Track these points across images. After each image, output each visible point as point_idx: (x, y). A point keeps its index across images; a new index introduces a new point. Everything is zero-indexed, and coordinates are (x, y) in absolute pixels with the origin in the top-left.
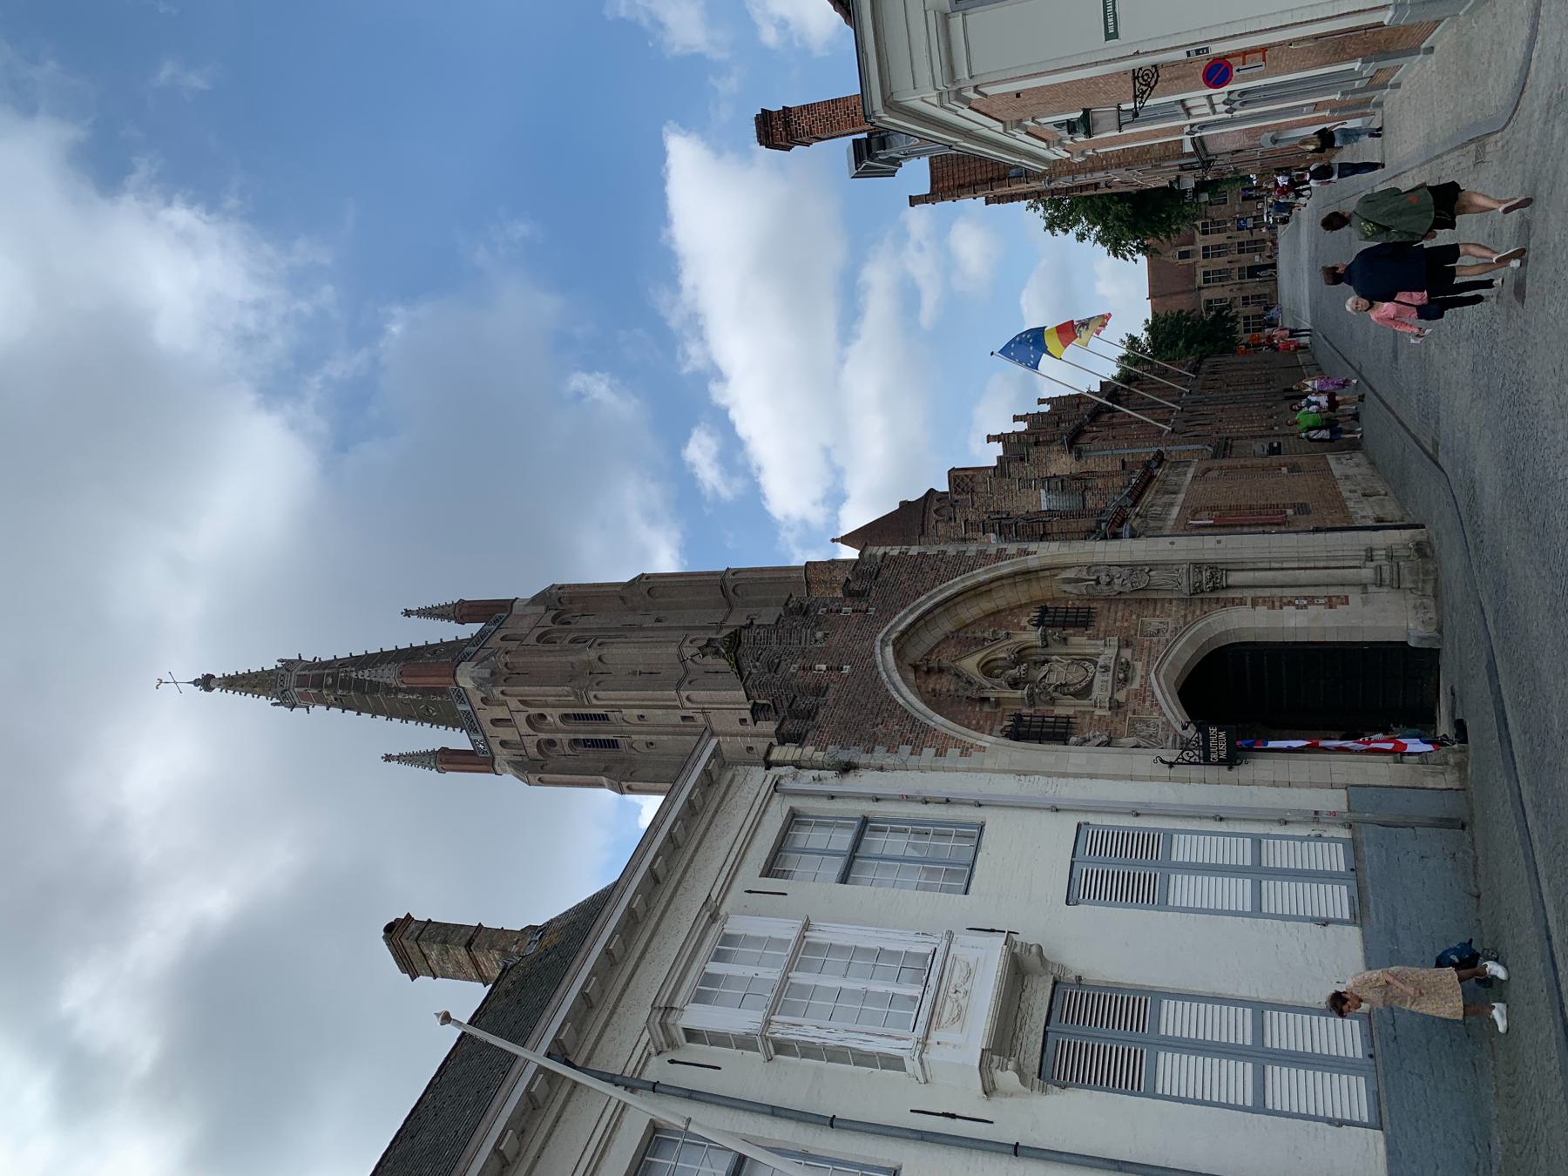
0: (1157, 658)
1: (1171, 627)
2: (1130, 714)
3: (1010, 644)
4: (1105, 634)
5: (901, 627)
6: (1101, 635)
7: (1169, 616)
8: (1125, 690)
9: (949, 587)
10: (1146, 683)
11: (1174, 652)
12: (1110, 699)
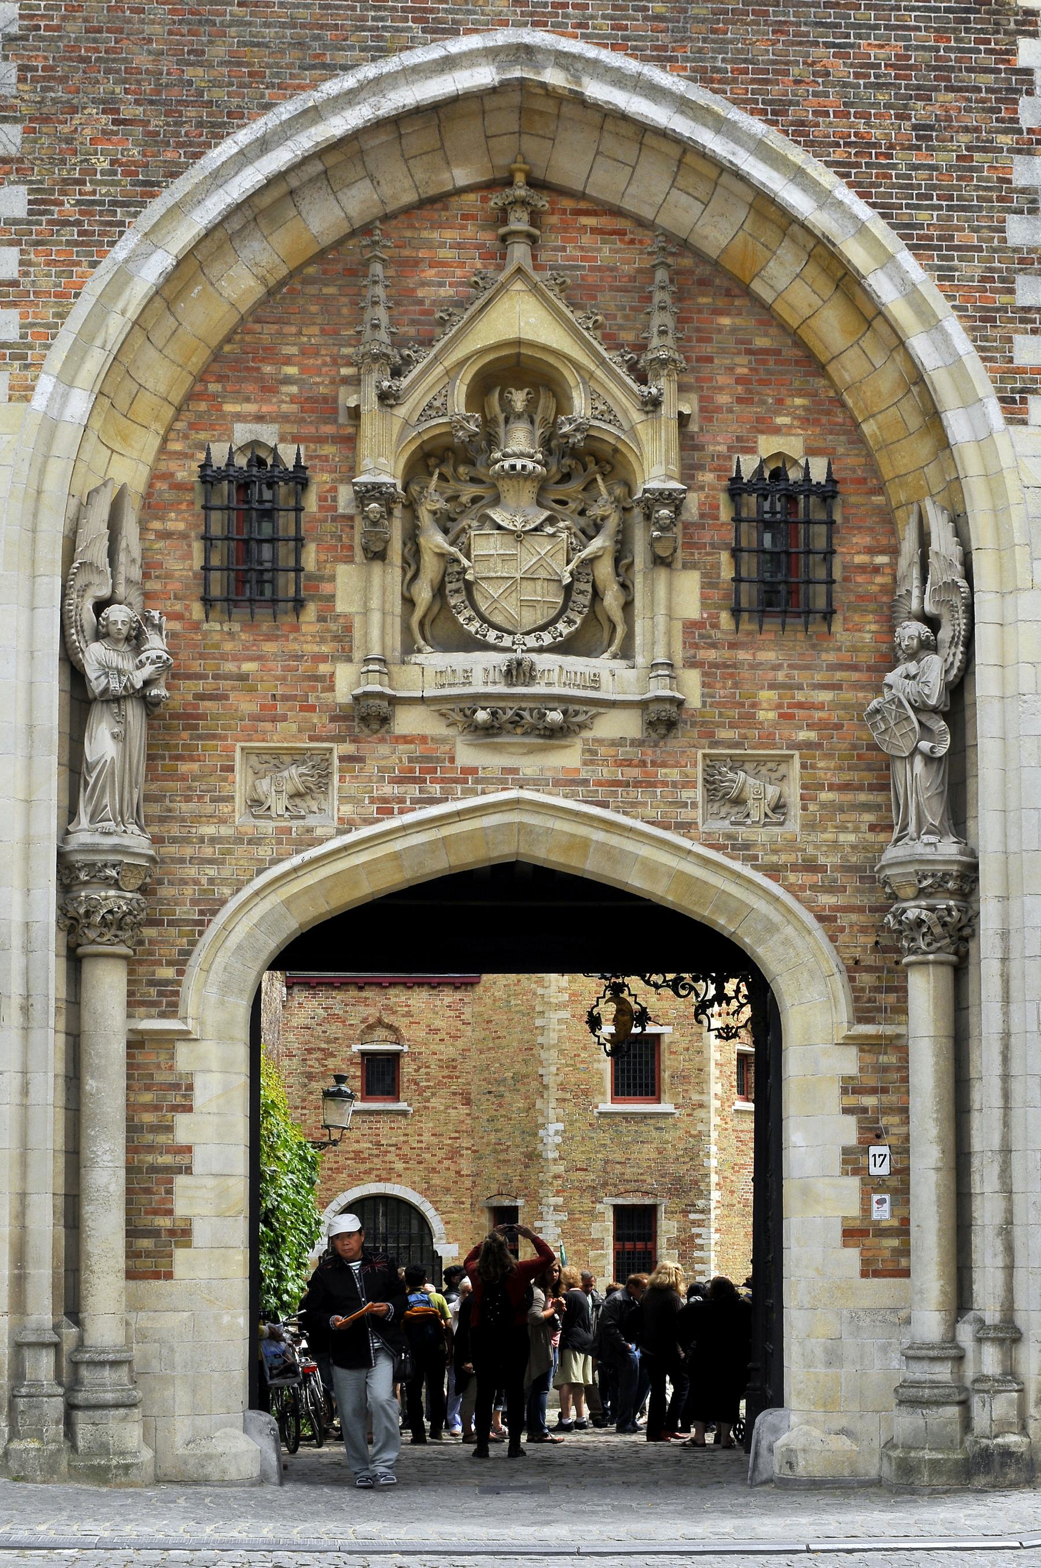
0: (604, 805)
1: (761, 835)
2: (339, 749)
3: (625, 412)
4: (715, 665)
5: (596, 90)
6: (712, 655)
7: (810, 826)
8: (451, 732)
9: (823, 197)
10: (477, 781)
11: (629, 845)
12: (394, 701)
